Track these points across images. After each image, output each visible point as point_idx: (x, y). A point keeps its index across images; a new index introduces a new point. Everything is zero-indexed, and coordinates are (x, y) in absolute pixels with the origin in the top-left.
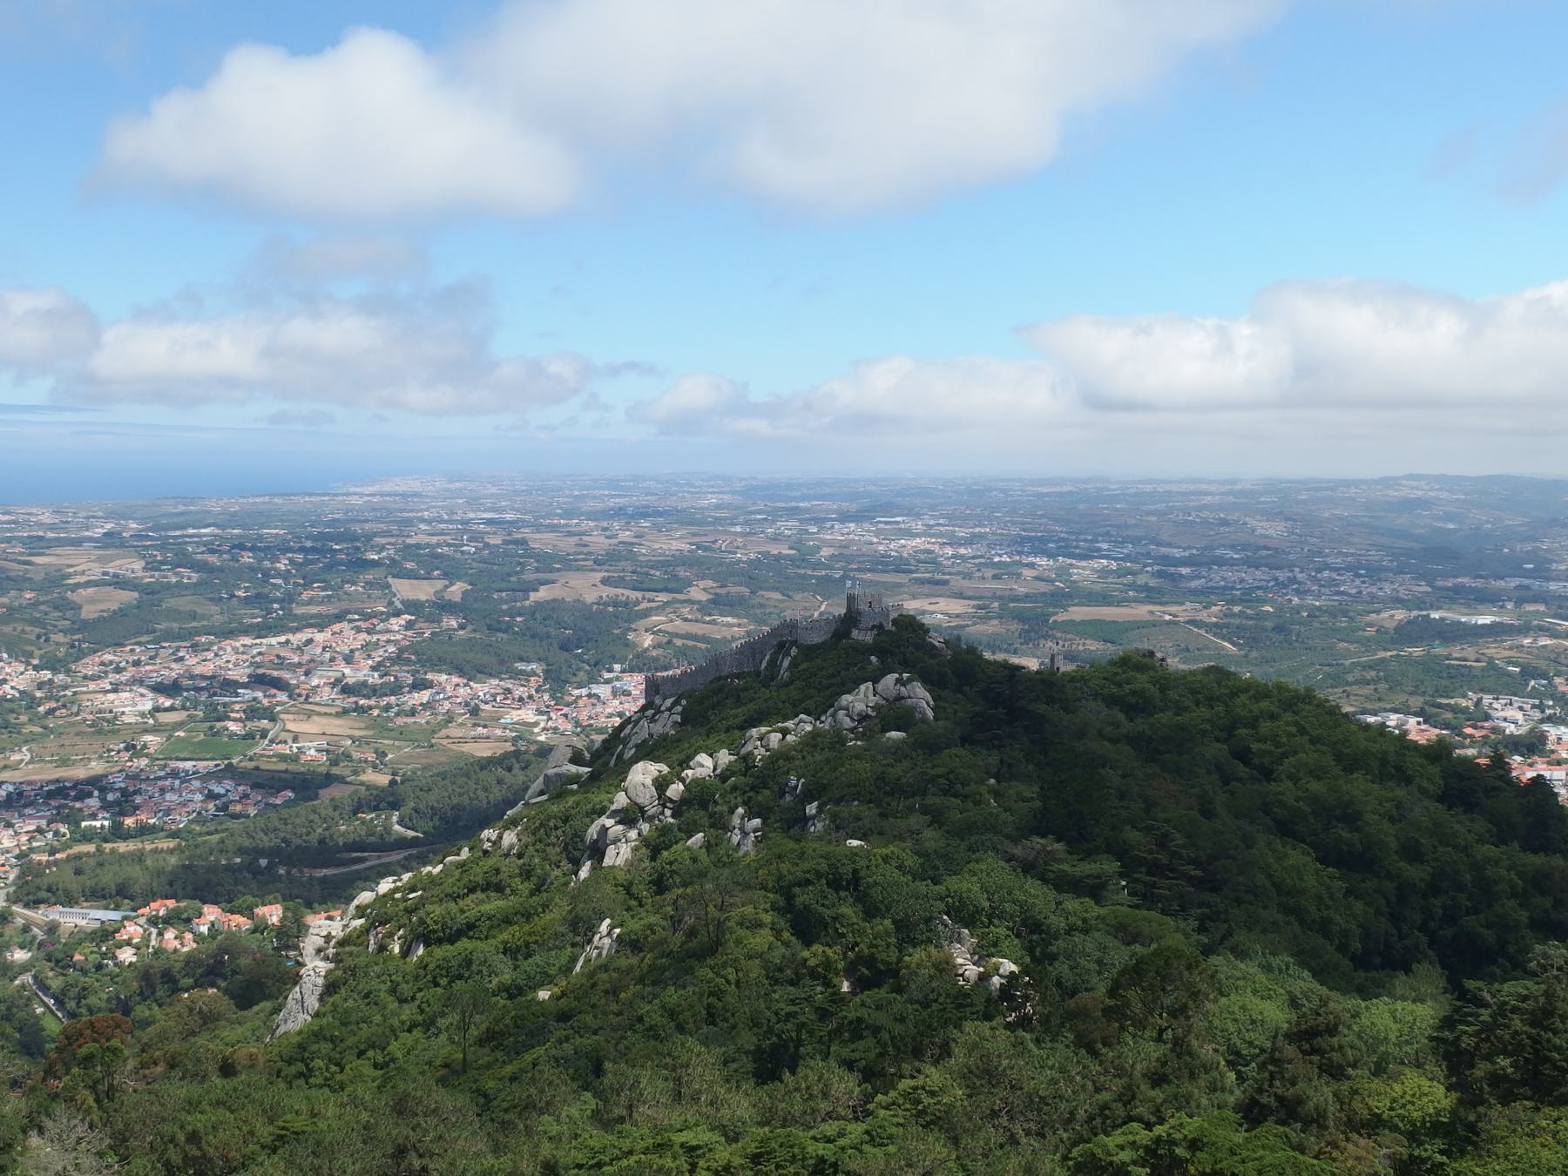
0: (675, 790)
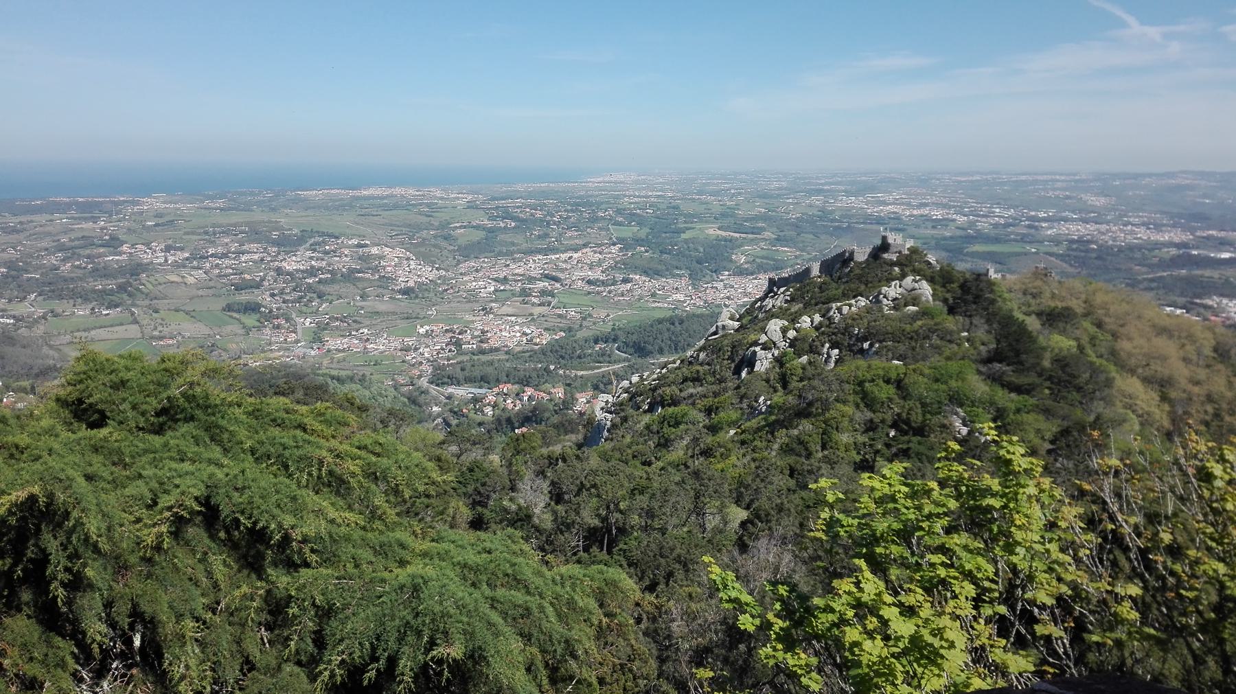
0: (792, 334)
